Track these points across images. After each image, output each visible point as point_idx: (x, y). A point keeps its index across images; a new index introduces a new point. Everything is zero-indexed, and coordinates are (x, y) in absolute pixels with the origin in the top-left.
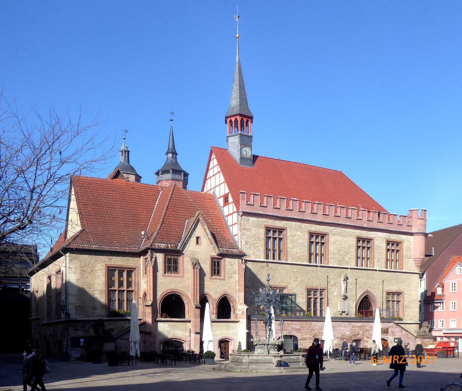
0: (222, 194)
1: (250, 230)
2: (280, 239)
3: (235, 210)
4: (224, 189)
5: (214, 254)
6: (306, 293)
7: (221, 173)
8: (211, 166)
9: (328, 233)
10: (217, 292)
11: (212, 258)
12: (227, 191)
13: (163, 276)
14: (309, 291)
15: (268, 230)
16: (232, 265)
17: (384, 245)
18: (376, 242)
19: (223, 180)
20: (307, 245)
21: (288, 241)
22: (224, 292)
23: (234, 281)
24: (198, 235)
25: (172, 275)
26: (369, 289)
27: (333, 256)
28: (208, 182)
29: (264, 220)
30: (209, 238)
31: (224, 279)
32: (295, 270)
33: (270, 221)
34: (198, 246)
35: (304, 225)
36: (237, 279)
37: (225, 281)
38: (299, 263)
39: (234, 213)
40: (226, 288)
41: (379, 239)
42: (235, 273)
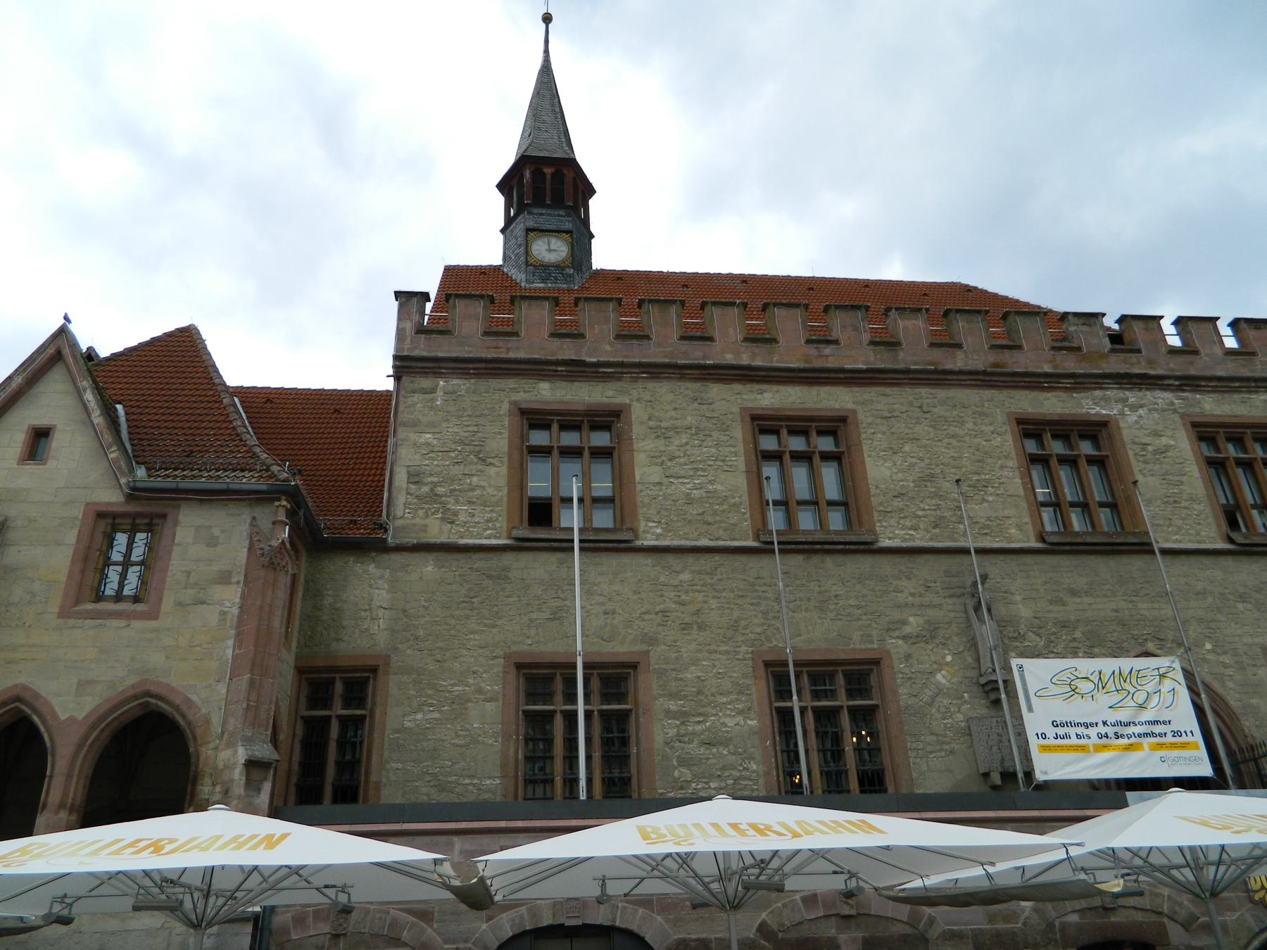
1: (433, 425)
5: (111, 497)
6: (759, 690)
9: (854, 412)
10: (90, 682)
14: (777, 675)
15: (535, 418)
16: (212, 543)
20: (742, 467)
21: (640, 458)
22: (133, 680)
23: (214, 619)
27: (898, 503)
29: (511, 383)
31: (153, 615)
32: (686, 576)
34: (31, 468)
35: (716, 391)
36: (235, 611)
37: (153, 624)
38: (704, 542)
40: (156, 659)
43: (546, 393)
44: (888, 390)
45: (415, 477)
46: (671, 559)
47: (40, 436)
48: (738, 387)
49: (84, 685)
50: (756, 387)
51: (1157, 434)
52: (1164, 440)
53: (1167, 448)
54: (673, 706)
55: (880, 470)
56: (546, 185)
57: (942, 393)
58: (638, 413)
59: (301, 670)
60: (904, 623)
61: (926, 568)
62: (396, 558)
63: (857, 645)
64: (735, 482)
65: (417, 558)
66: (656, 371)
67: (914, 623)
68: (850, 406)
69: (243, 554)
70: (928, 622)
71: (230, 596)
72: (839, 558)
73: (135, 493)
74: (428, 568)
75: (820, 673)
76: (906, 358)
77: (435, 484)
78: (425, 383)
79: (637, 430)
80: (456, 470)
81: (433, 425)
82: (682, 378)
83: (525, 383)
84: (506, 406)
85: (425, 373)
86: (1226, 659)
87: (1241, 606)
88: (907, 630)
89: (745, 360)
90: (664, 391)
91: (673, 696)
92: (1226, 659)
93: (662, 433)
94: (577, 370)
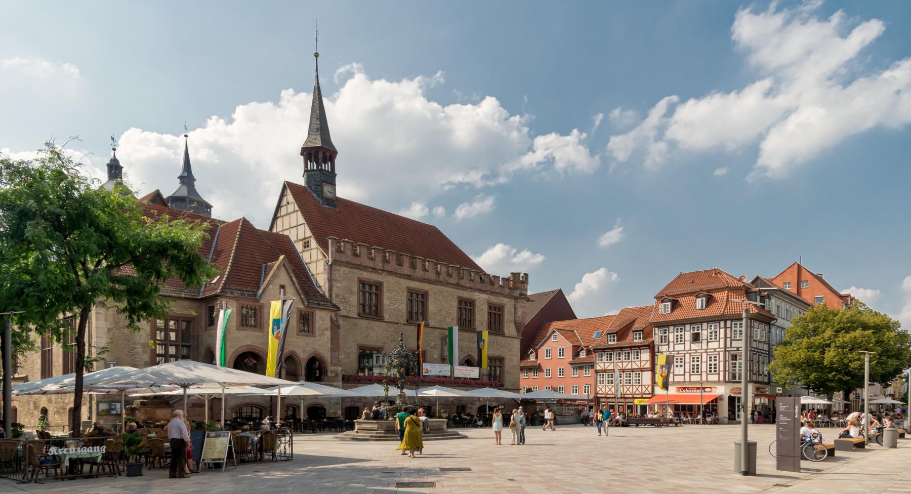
0: (301, 236)
3: (320, 257)
4: (304, 231)
5: (301, 306)
7: (299, 213)
8: (284, 202)
11: (300, 311)
12: (309, 233)
15: (362, 283)
16: (323, 320)
17: (485, 308)
18: (478, 304)
19: (302, 220)
21: (385, 298)
24: (283, 283)
28: (279, 221)
29: (356, 271)
30: (296, 288)
35: (402, 281)
39: (317, 261)
41: (482, 300)
42: (326, 329)
45: (337, 296)
55: (432, 307)
58: (385, 285)
66: (390, 273)
69: (329, 324)
73: (308, 306)
78: (338, 268)
79: (385, 290)
80: (346, 295)
81: (340, 281)
83: (361, 272)
84: (356, 279)
93: (390, 291)
94: (374, 270)
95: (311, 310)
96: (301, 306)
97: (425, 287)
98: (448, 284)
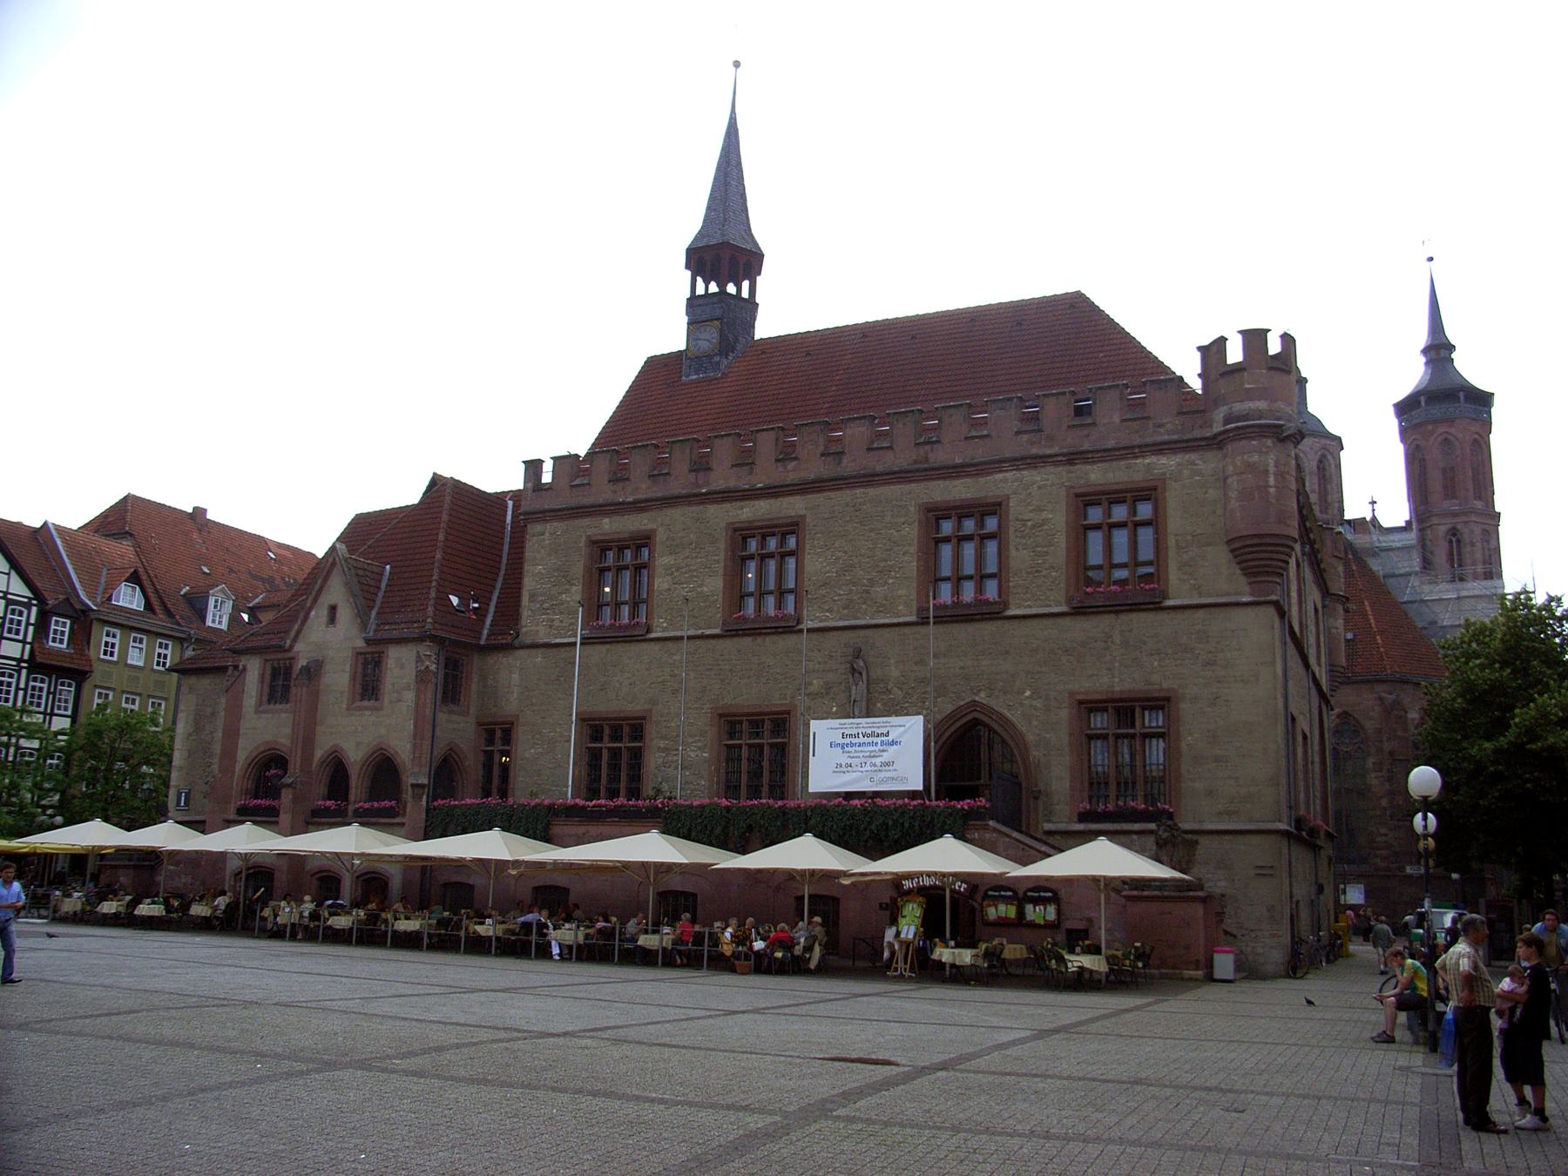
2: (639, 568)
9: (803, 517)
13: (257, 712)
16: (402, 667)
17: (1058, 518)
20: (721, 571)
21: (659, 571)
24: (332, 602)
25: (278, 706)
26: (982, 697)
29: (586, 521)
33: (606, 520)
34: (331, 629)
35: (712, 509)
40: (383, 731)
42: (407, 687)
43: (608, 526)
44: (832, 494)
45: (533, 596)
46: (670, 644)
47: (333, 609)
48: (727, 506)
49: (358, 744)
50: (739, 504)
51: (1040, 509)
52: (1044, 515)
53: (1045, 521)
54: (662, 744)
56: (724, 254)
57: (872, 492)
58: (661, 536)
59: (479, 724)
60: (811, 684)
61: (832, 640)
62: (521, 653)
63: (777, 702)
64: (714, 585)
65: (534, 651)
67: (817, 684)
68: (802, 512)
70: (827, 683)
71: (410, 696)
72: (775, 638)
73: (368, 641)
74: (538, 658)
75: (756, 721)
76: (848, 466)
77: (543, 602)
78: (538, 528)
79: (659, 548)
82: (690, 504)
84: (583, 539)
85: (537, 521)
86: (1038, 704)
87: (1064, 659)
88: (811, 689)
89: (732, 484)
90: (677, 515)
91: (664, 738)
92: (1038, 704)
95: (378, 648)
96: (360, 643)
97: (794, 506)
98: (869, 479)
